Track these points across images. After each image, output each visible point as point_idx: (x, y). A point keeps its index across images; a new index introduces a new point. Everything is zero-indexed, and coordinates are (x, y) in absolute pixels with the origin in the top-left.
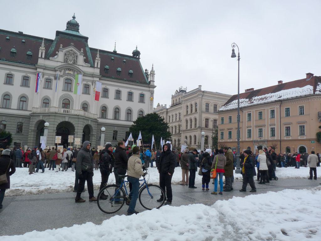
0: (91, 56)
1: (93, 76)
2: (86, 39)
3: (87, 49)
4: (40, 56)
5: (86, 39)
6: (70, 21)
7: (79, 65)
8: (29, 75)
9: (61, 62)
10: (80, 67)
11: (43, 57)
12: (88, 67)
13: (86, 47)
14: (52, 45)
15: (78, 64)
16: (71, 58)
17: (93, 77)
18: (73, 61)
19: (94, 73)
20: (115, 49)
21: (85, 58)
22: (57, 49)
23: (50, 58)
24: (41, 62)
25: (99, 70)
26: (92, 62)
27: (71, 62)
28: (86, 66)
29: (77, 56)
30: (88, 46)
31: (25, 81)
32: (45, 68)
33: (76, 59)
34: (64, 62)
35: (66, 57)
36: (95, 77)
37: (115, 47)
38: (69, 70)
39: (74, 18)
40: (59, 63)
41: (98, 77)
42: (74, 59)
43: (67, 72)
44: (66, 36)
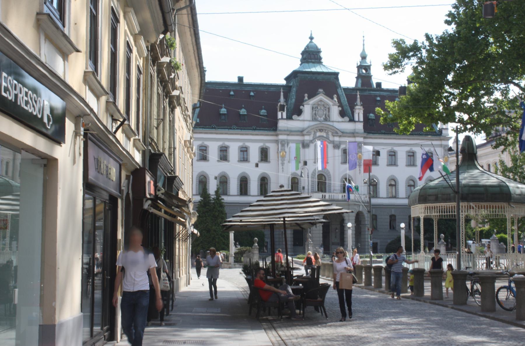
0: (347, 102)
1: (353, 134)
2: (336, 74)
3: (339, 91)
4: (279, 116)
5: (336, 74)
6: (307, 46)
7: (333, 121)
8: (268, 145)
9: (309, 121)
10: (336, 125)
11: (285, 116)
12: (345, 122)
13: (338, 88)
14: (291, 94)
15: (332, 120)
16: (321, 112)
17: (355, 137)
18: (324, 116)
19: (355, 130)
20: (364, 50)
21: (340, 109)
22: (300, 102)
23: (295, 117)
24: (282, 124)
25: (362, 124)
26: (350, 112)
27: (322, 119)
28: (343, 122)
29: (329, 108)
30: (340, 85)
31: (264, 155)
32: (290, 132)
33: (327, 113)
34: (313, 120)
35: (314, 112)
36: (358, 136)
37: (364, 45)
38: (321, 130)
39: (311, 38)
40: (306, 122)
41: (361, 137)
42: (325, 112)
43: (318, 134)
44: (307, 75)
